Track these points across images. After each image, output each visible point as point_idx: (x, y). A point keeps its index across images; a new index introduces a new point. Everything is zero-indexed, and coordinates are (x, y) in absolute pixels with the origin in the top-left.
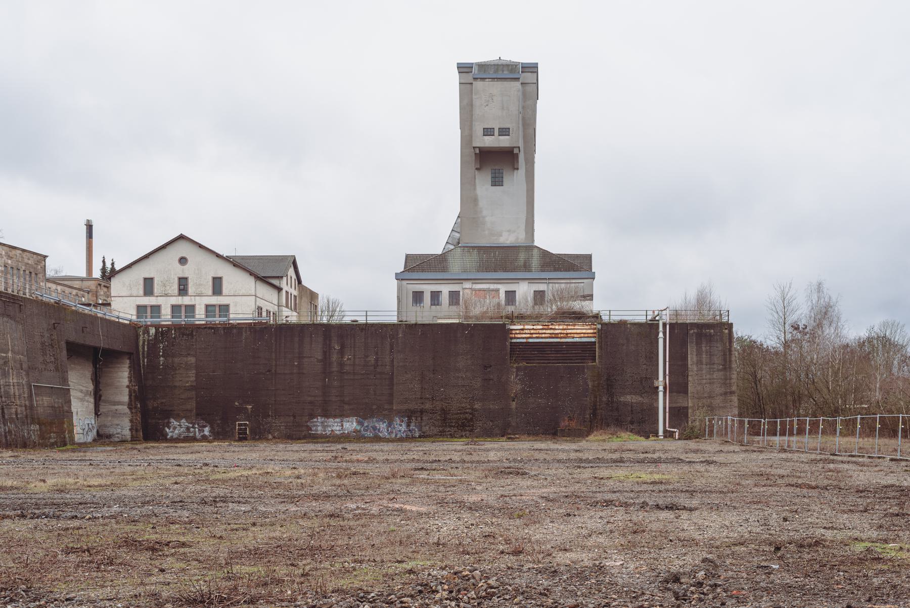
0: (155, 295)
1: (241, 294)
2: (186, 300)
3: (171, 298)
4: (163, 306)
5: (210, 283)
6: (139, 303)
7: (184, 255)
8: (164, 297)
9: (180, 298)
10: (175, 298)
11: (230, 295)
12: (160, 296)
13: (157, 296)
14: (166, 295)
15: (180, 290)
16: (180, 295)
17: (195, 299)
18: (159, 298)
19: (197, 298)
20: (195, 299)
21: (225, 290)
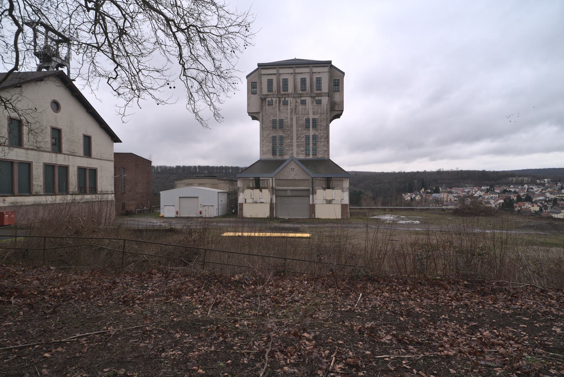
0: (25, 147)
1: (105, 159)
2: (60, 160)
3: (44, 153)
4: (34, 164)
5: (82, 142)
6: (47, 161)
7: (60, 102)
8: (36, 152)
9: (54, 155)
10: (48, 154)
11: (98, 158)
12: (32, 149)
13: (27, 149)
14: (38, 149)
15: (53, 145)
16: (53, 151)
17: (68, 158)
18: (29, 151)
19: (71, 157)
20: (68, 158)
21: (94, 153)
